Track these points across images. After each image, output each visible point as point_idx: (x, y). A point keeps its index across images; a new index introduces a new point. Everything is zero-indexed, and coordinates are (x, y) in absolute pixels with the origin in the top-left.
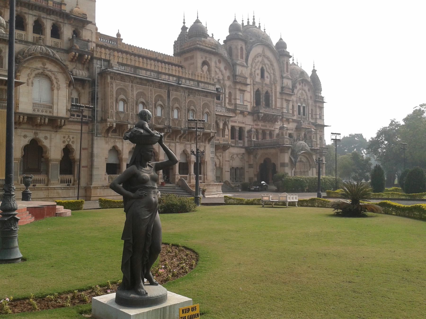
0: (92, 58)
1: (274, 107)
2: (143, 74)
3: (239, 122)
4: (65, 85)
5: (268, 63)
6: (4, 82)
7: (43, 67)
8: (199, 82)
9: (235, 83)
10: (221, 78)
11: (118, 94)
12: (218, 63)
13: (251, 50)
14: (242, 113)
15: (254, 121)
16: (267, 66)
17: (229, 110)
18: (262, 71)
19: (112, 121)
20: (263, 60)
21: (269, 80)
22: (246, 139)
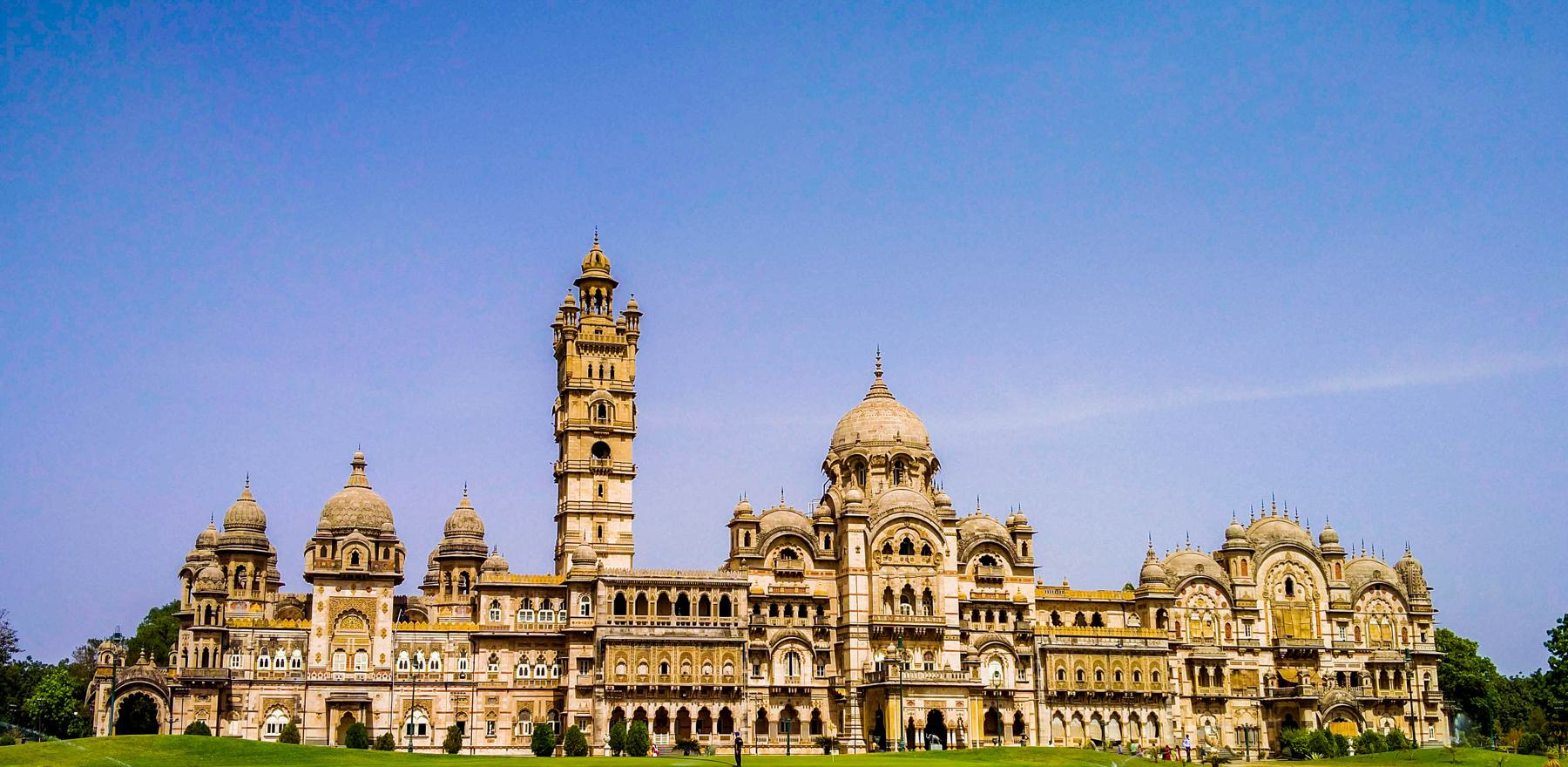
9: (1234, 612)
10: (1211, 606)
14: (1250, 651)
17: (1226, 649)
18: (1289, 584)
19: (1053, 689)
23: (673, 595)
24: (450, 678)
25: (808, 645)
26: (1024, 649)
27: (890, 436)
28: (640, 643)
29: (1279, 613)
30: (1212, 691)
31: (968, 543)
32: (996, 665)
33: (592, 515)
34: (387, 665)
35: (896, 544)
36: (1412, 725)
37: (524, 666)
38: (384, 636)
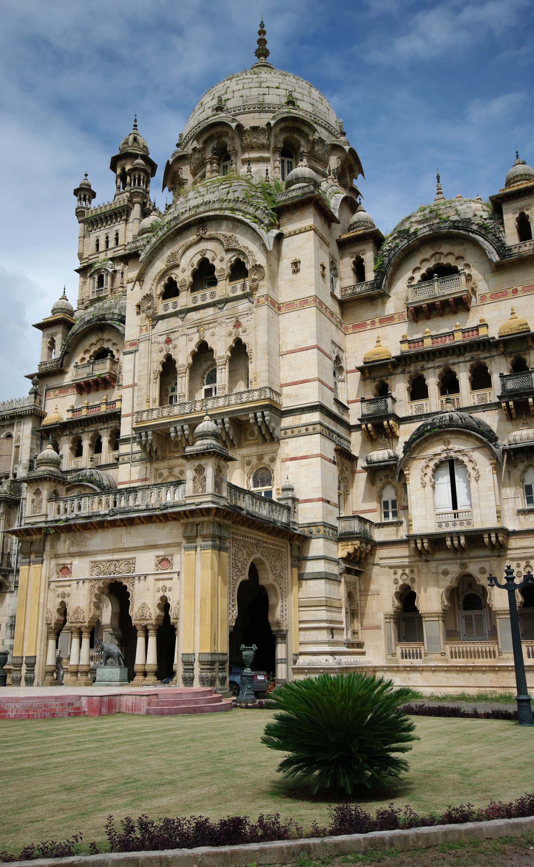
4: (490, 468)
6: (214, 512)
7: (445, 448)
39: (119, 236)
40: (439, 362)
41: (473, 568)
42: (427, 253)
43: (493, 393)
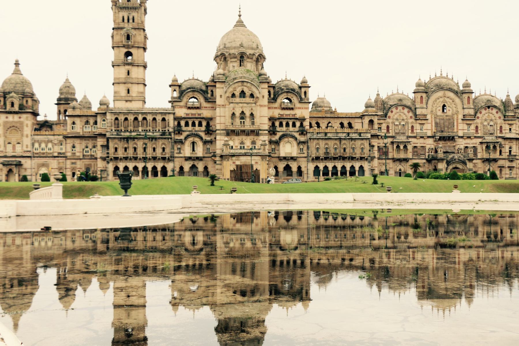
0: (307, 133)
1: (455, 131)
2: (329, 135)
3: (420, 144)
5: (451, 101)
8: (360, 133)
10: (405, 118)
11: (316, 145)
12: (402, 110)
13: (430, 96)
15: (435, 141)
16: (448, 103)
17: (411, 137)
18: (444, 106)
19: (314, 156)
20: (444, 99)
21: (451, 112)
22: (427, 154)
23: (140, 118)
24: (56, 154)
25: (201, 138)
26: (302, 139)
27: (238, 44)
28: (124, 138)
29: (438, 121)
30: (402, 156)
31: (278, 91)
32: (288, 146)
33: (125, 83)
34: (29, 149)
35: (237, 93)
36: (501, 171)
37: (87, 149)
38: (27, 136)
39: (135, 18)
40: (286, 120)
41: (289, 163)
42: (285, 94)
43: (297, 129)
